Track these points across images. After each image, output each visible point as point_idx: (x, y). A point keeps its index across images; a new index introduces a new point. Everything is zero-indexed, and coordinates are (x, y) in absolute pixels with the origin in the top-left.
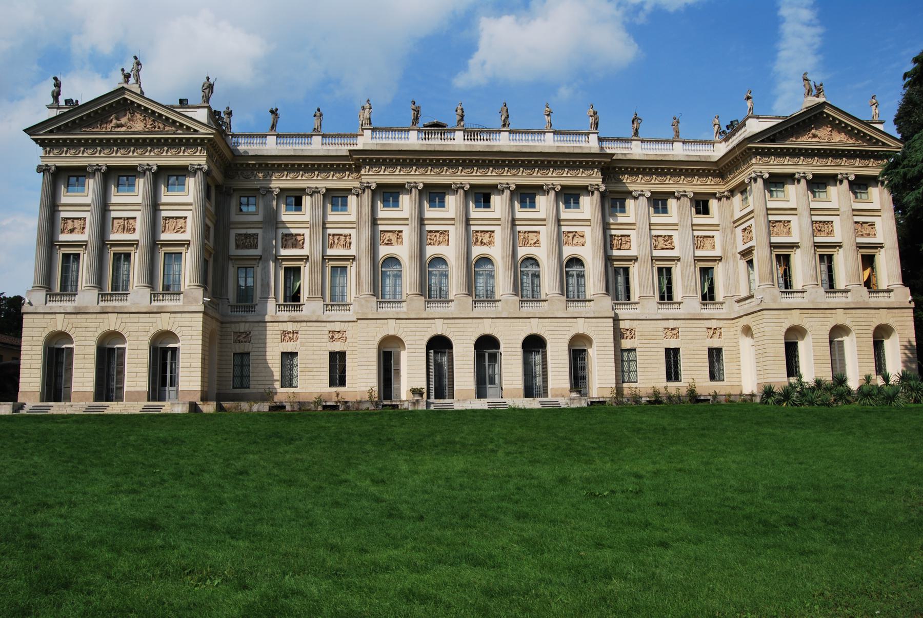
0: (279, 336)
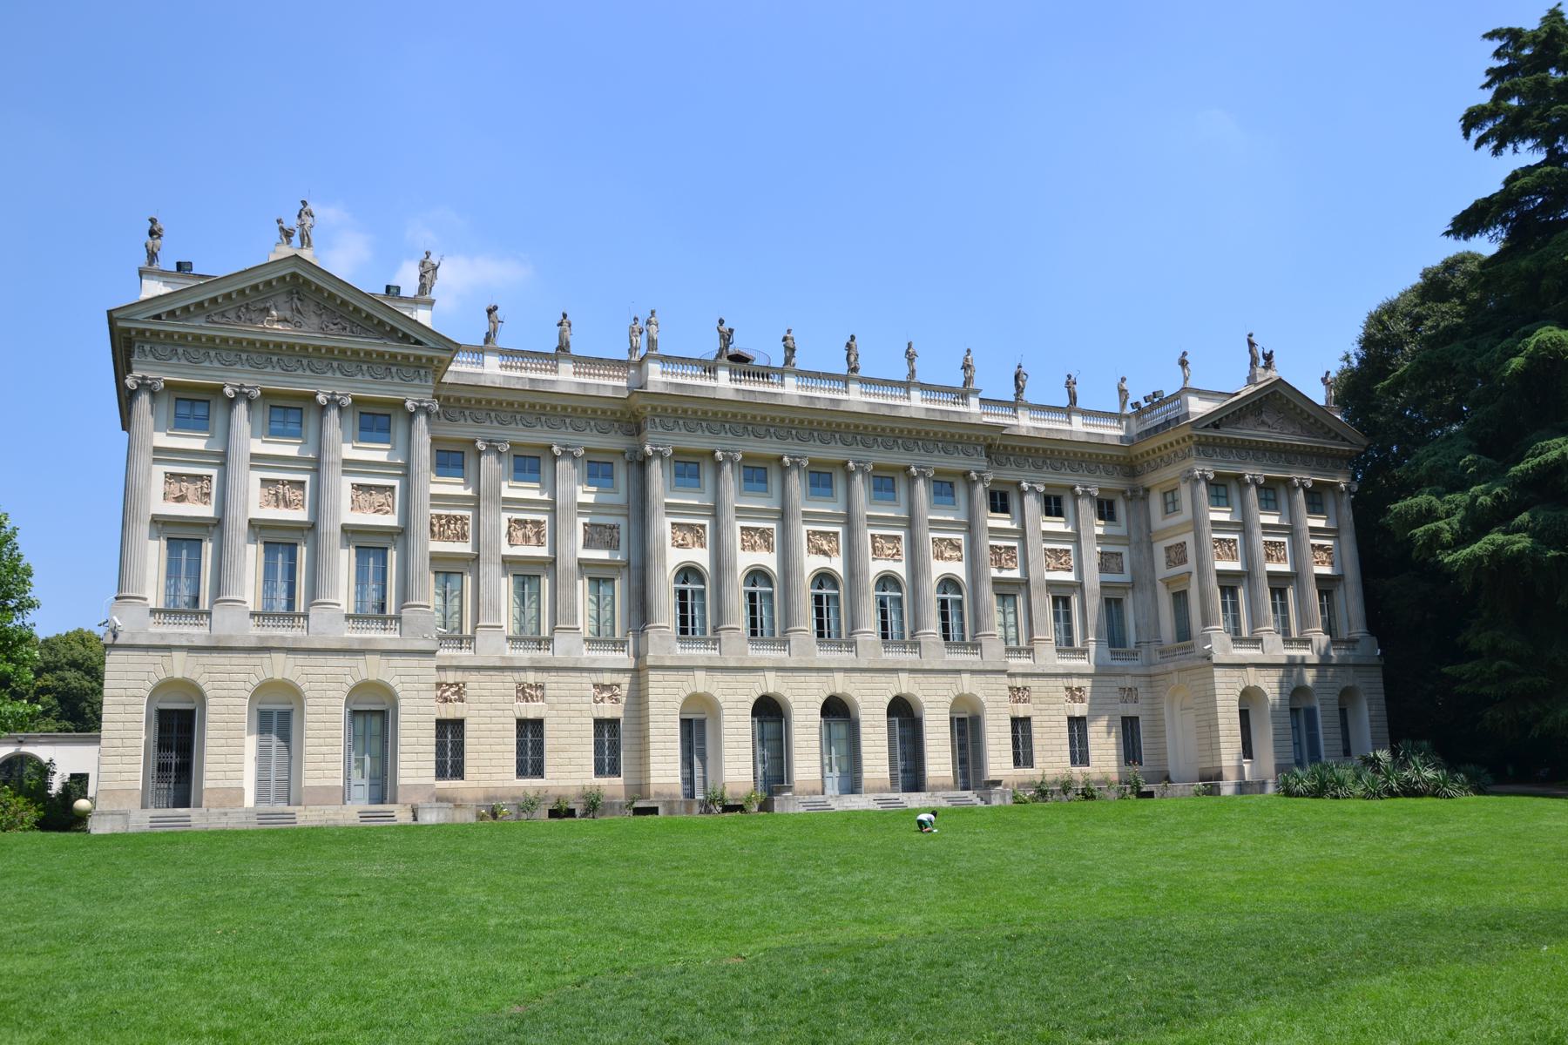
0: (469, 692)
